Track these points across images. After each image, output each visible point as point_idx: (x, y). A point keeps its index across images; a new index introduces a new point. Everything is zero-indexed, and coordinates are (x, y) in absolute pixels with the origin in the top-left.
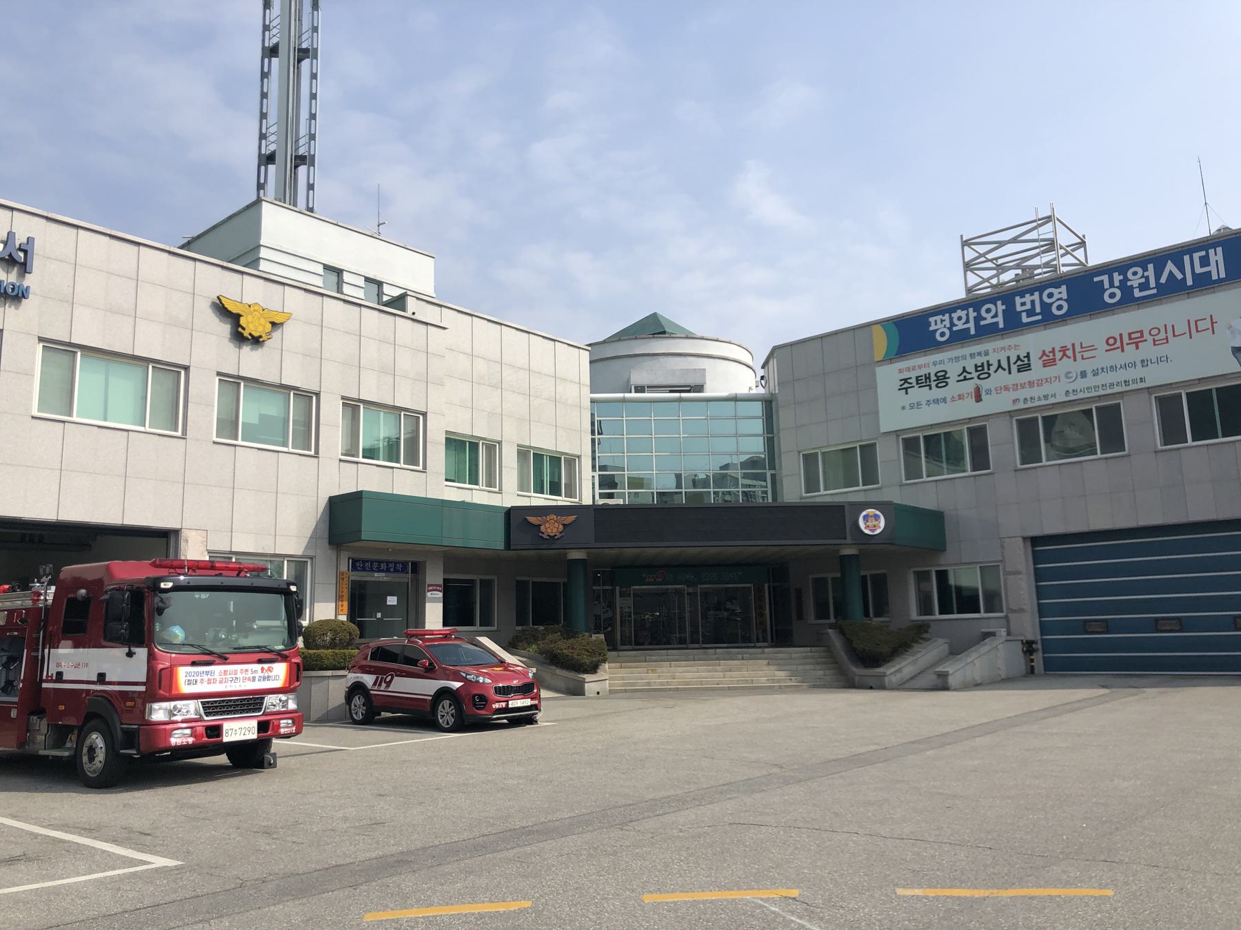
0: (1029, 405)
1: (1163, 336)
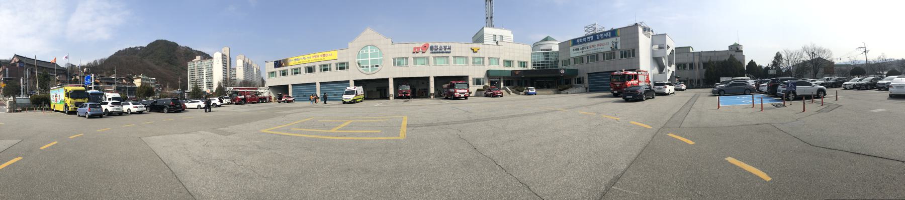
1: (603, 45)
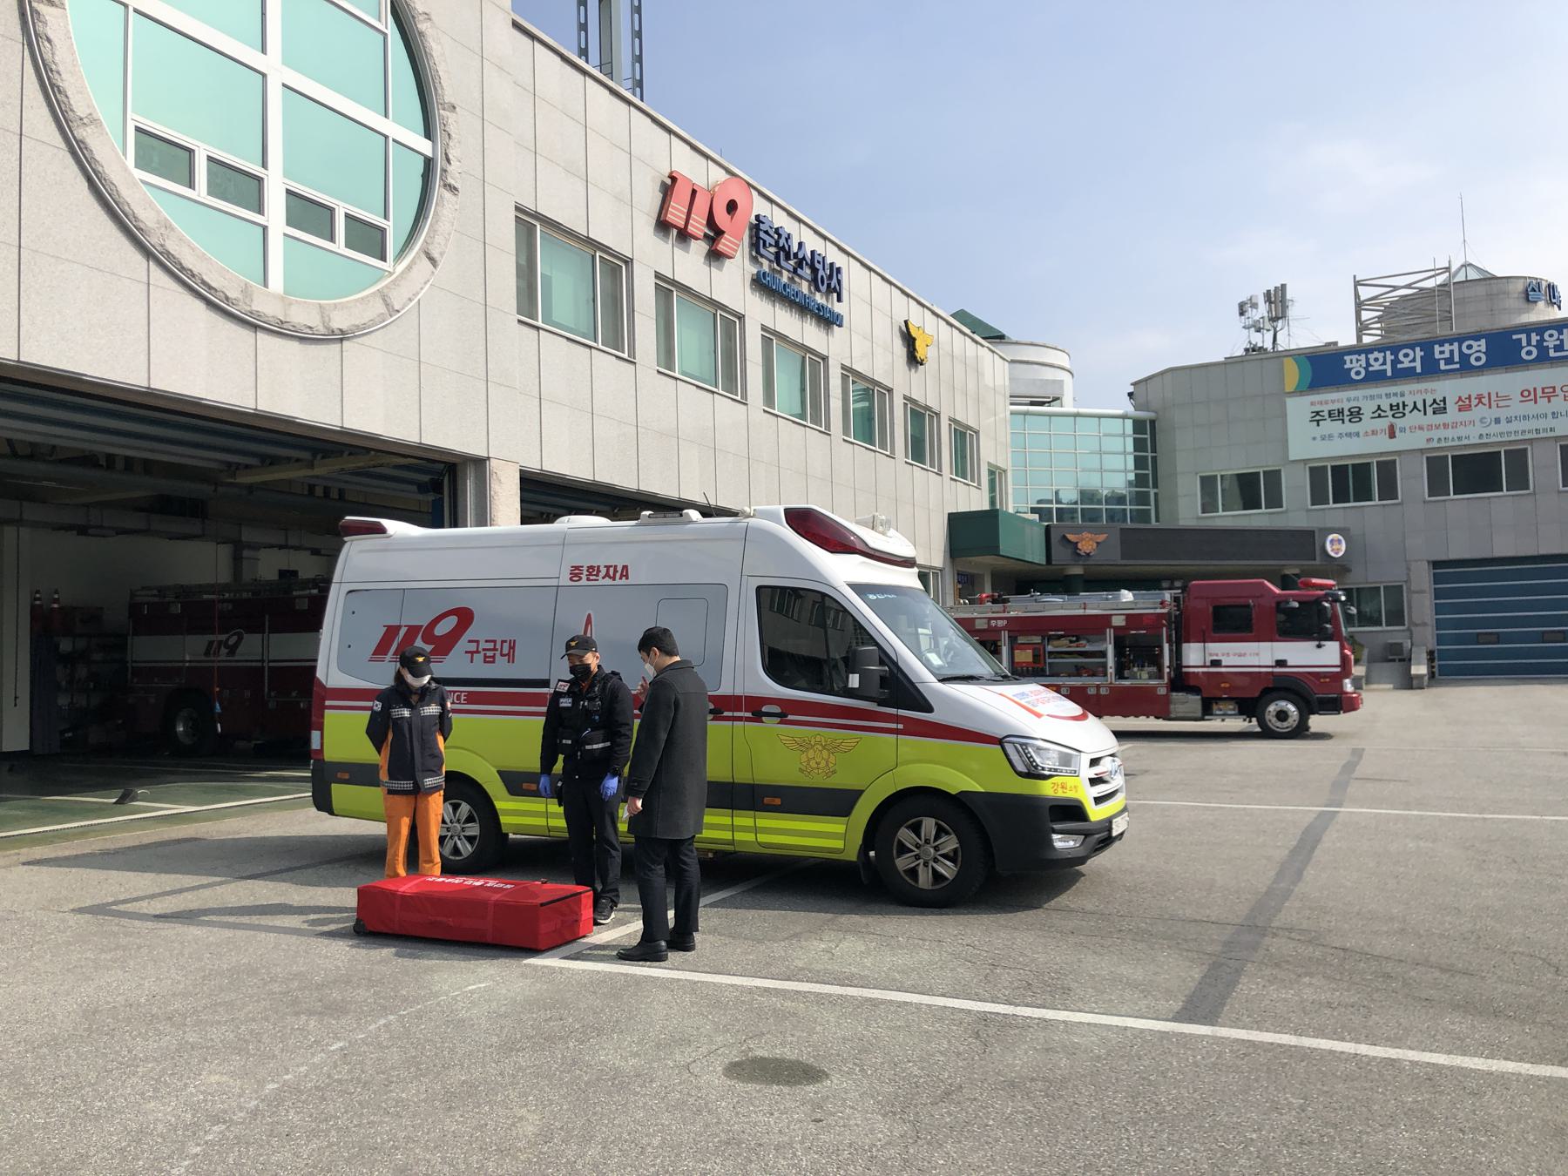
0: (1443, 444)
